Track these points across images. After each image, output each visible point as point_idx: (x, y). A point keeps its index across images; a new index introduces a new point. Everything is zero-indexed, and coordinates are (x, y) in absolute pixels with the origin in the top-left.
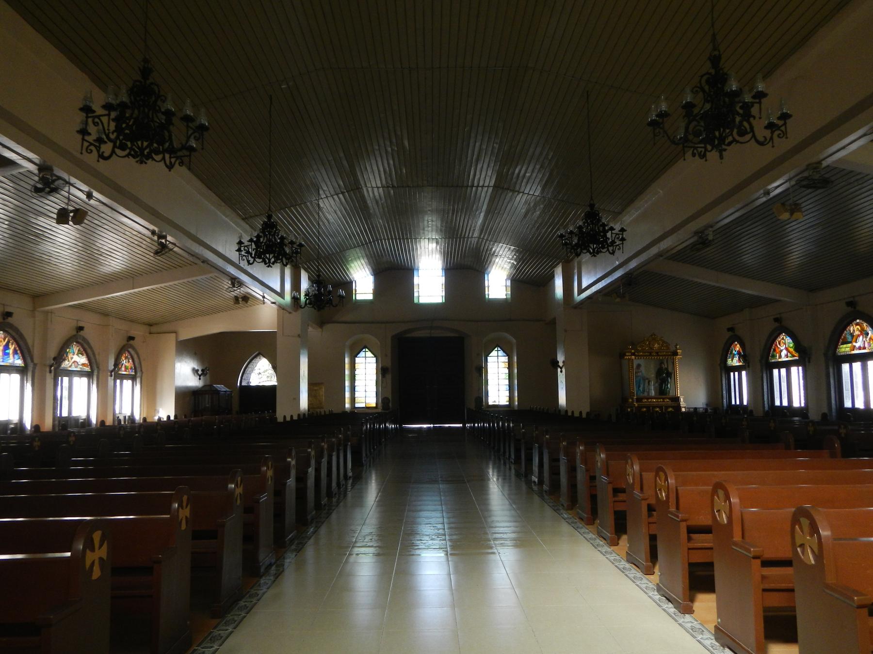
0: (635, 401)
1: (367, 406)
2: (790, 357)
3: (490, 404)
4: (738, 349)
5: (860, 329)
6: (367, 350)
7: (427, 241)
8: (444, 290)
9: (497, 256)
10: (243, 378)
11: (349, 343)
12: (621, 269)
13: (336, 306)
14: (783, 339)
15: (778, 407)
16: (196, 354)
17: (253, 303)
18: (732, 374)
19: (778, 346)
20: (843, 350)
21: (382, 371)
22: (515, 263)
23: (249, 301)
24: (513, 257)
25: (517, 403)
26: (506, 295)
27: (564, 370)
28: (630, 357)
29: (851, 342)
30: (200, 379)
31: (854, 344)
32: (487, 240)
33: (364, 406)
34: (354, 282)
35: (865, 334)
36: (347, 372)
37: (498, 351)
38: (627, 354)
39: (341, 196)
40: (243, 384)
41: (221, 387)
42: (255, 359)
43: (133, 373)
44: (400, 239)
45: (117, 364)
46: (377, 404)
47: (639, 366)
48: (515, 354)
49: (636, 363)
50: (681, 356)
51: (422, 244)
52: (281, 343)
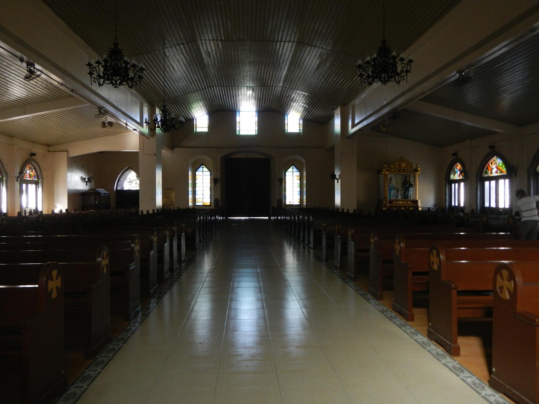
0: (388, 202)
1: (204, 204)
2: (499, 173)
3: (287, 204)
4: (458, 168)
6: (204, 166)
7: (246, 88)
8: (257, 126)
9: (295, 101)
10: (118, 184)
11: (191, 161)
12: (389, 106)
13: (178, 129)
14: (494, 160)
15: (487, 208)
16: (83, 167)
17: (122, 131)
18: (453, 185)
21: (214, 181)
22: (307, 107)
23: (113, 126)
24: (306, 102)
25: (305, 204)
26: (299, 130)
27: (339, 181)
28: (385, 173)
30: (87, 185)
32: (289, 88)
33: (202, 204)
34: (195, 119)
37: (293, 168)
38: (384, 170)
39: (182, 46)
40: (118, 188)
41: (102, 191)
42: (126, 172)
43: (37, 180)
44: (226, 86)
45: (22, 172)
47: (391, 179)
48: (305, 171)
49: (389, 176)
50: (420, 173)
51: (243, 91)
52: (142, 159)
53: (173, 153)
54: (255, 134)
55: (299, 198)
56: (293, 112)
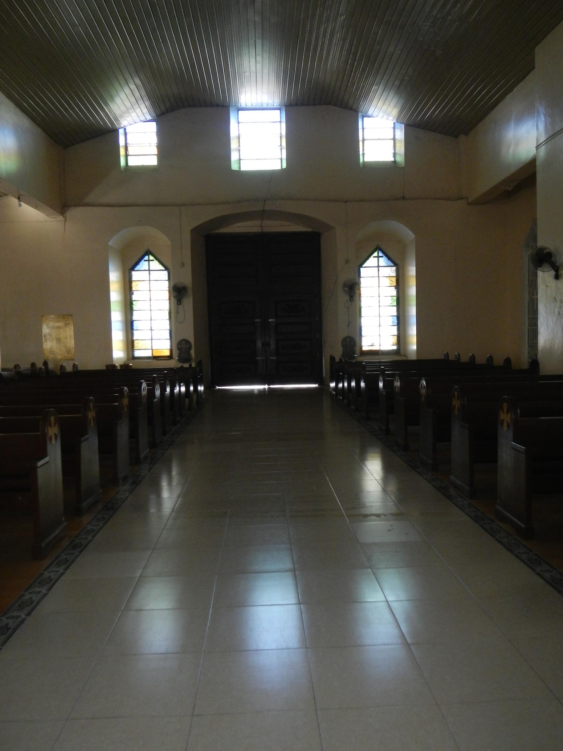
1: (155, 355)
3: (364, 348)
6: (151, 258)
25: (414, 347)
26: (395, 155)
33: (150, 355)
34: (121, 131)
36: (115, 296)
37: (378, 257)
46: (171, 351)
53: (66, 220)
54: (279, 168)
55: (396, 333)
56: (380, 103)
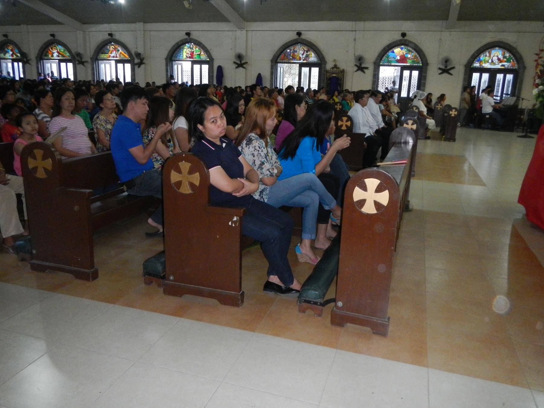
2: (61, 57)
5: (114, 47)
19: (51, 50)
20: (102, 57)
29: (107, 53)
31: (110, 54)
35: (117, 50)
